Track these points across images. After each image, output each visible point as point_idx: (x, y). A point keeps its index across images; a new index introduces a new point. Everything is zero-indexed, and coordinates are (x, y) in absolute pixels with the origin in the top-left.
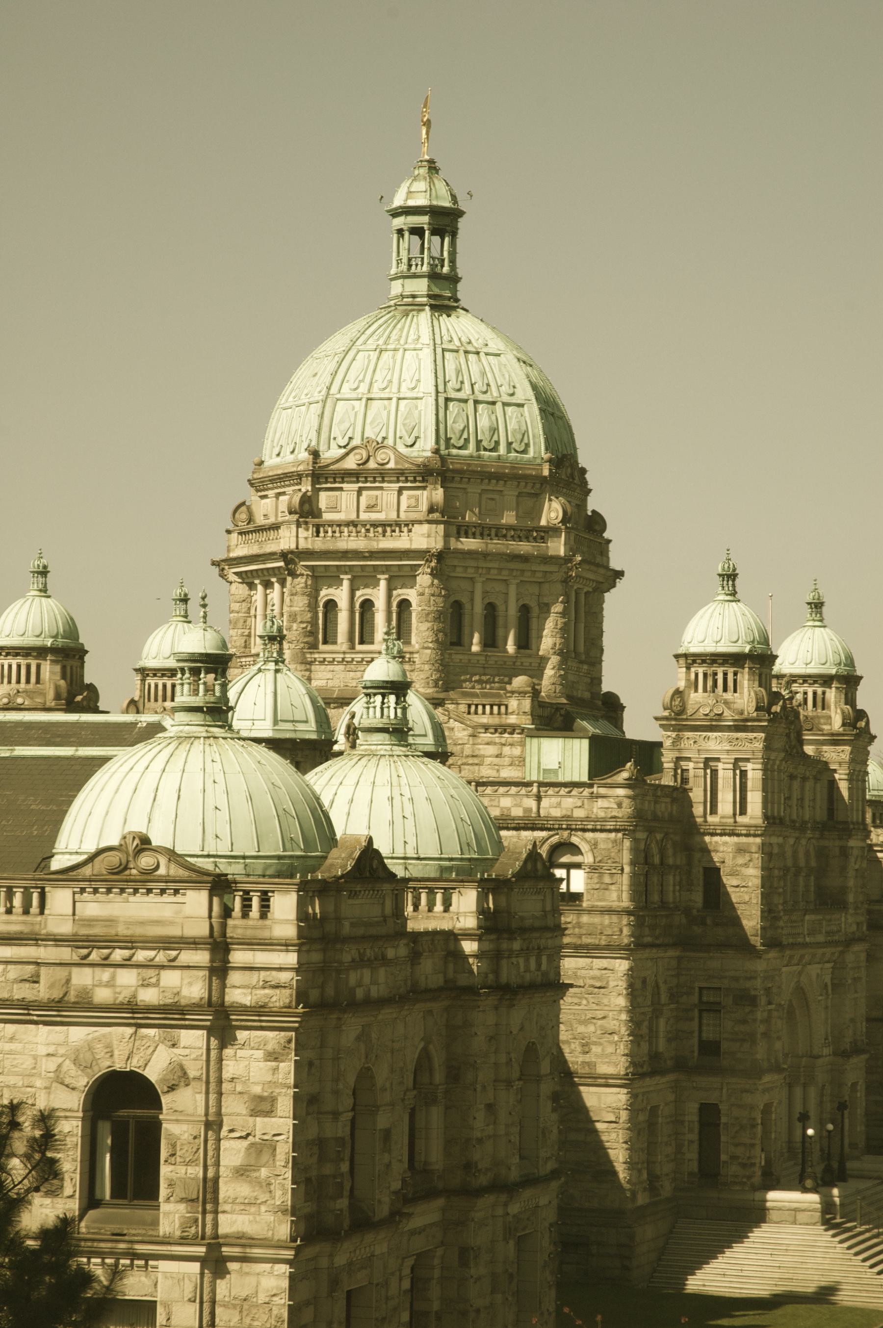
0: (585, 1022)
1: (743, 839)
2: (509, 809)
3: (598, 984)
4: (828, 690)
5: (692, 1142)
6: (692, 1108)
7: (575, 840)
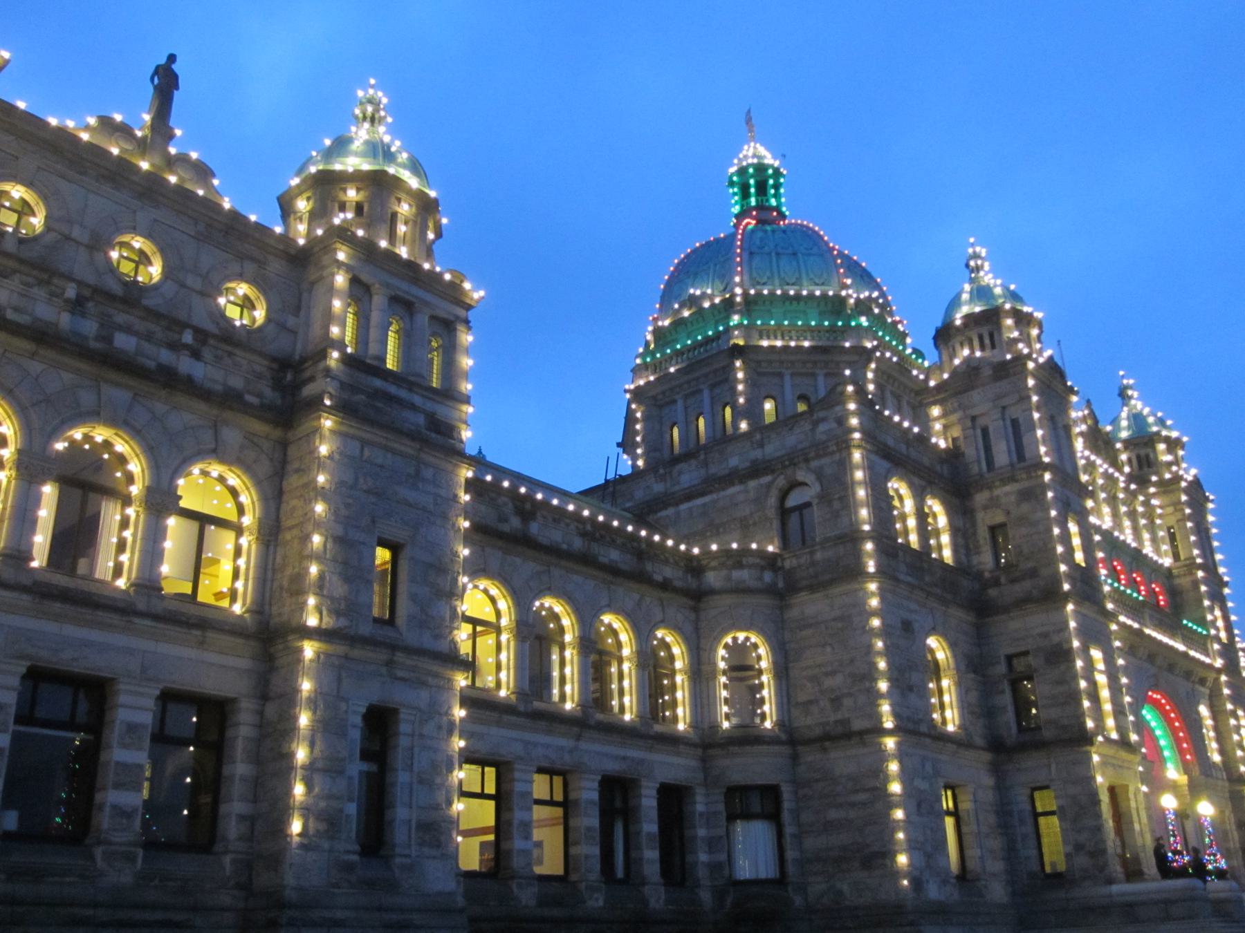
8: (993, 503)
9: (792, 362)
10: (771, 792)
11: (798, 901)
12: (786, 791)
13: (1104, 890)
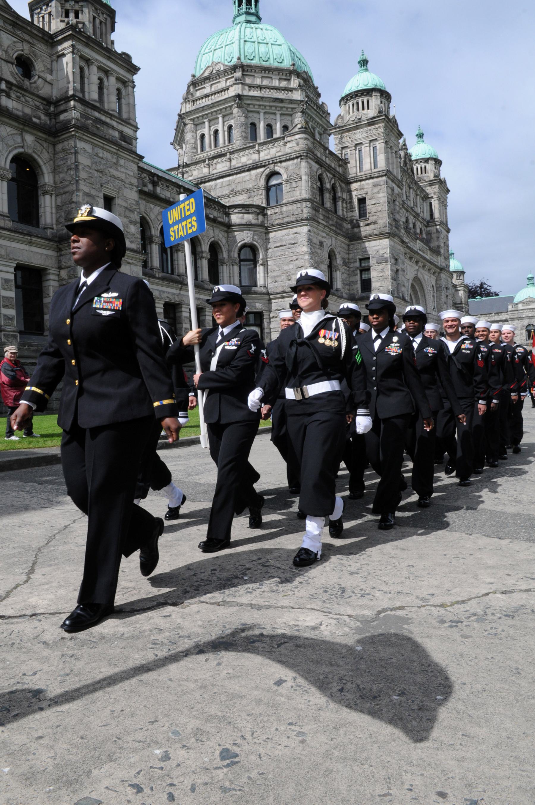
0: (288, 264)
1: (376, 180)
3: (293, 242)
4: (427, 165)
7: (277, 169)
9: (265, 106)
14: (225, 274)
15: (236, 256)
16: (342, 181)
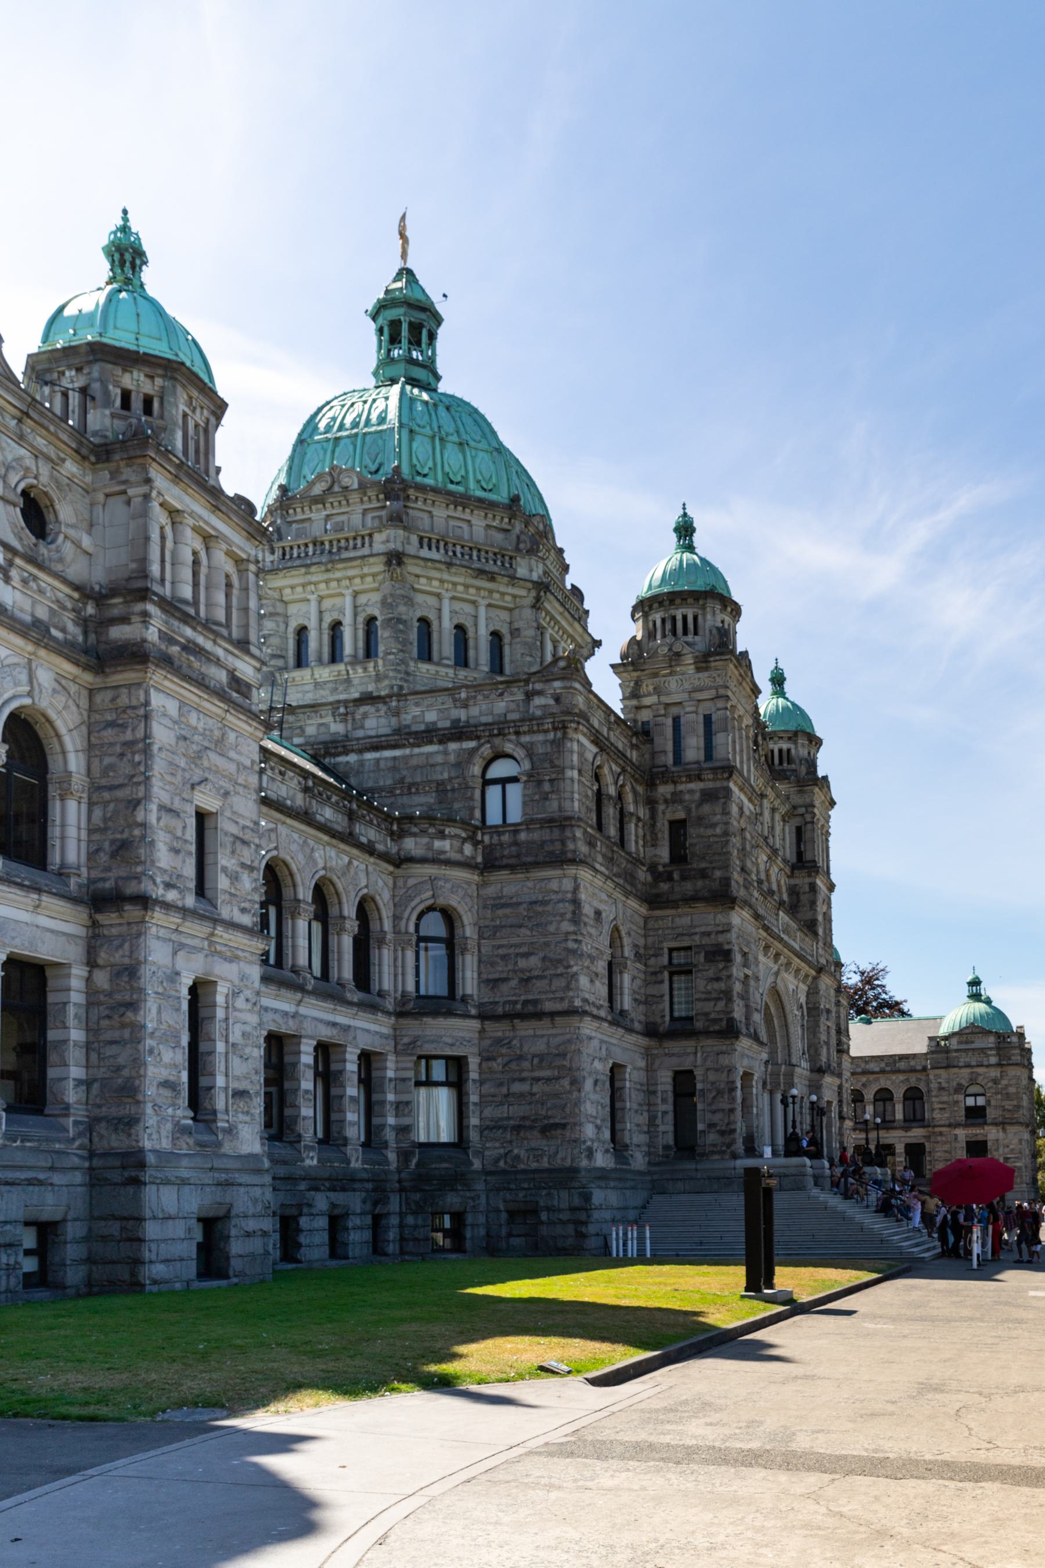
0: (526, 955)
2: (434, 723)
5: (665, 1113)
6: (665, 1080)
7: (509, 747)
8: (676, 798)
10: (457, 1065)
11: (477, 1165)
12: (473, 1062)
13: (731, 1164)
14: (386, 969)
15: (412, 928)
16: (636, 780)
